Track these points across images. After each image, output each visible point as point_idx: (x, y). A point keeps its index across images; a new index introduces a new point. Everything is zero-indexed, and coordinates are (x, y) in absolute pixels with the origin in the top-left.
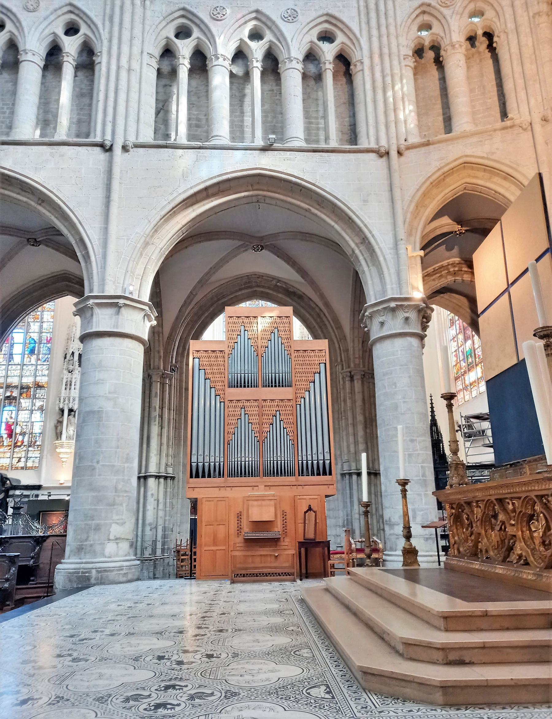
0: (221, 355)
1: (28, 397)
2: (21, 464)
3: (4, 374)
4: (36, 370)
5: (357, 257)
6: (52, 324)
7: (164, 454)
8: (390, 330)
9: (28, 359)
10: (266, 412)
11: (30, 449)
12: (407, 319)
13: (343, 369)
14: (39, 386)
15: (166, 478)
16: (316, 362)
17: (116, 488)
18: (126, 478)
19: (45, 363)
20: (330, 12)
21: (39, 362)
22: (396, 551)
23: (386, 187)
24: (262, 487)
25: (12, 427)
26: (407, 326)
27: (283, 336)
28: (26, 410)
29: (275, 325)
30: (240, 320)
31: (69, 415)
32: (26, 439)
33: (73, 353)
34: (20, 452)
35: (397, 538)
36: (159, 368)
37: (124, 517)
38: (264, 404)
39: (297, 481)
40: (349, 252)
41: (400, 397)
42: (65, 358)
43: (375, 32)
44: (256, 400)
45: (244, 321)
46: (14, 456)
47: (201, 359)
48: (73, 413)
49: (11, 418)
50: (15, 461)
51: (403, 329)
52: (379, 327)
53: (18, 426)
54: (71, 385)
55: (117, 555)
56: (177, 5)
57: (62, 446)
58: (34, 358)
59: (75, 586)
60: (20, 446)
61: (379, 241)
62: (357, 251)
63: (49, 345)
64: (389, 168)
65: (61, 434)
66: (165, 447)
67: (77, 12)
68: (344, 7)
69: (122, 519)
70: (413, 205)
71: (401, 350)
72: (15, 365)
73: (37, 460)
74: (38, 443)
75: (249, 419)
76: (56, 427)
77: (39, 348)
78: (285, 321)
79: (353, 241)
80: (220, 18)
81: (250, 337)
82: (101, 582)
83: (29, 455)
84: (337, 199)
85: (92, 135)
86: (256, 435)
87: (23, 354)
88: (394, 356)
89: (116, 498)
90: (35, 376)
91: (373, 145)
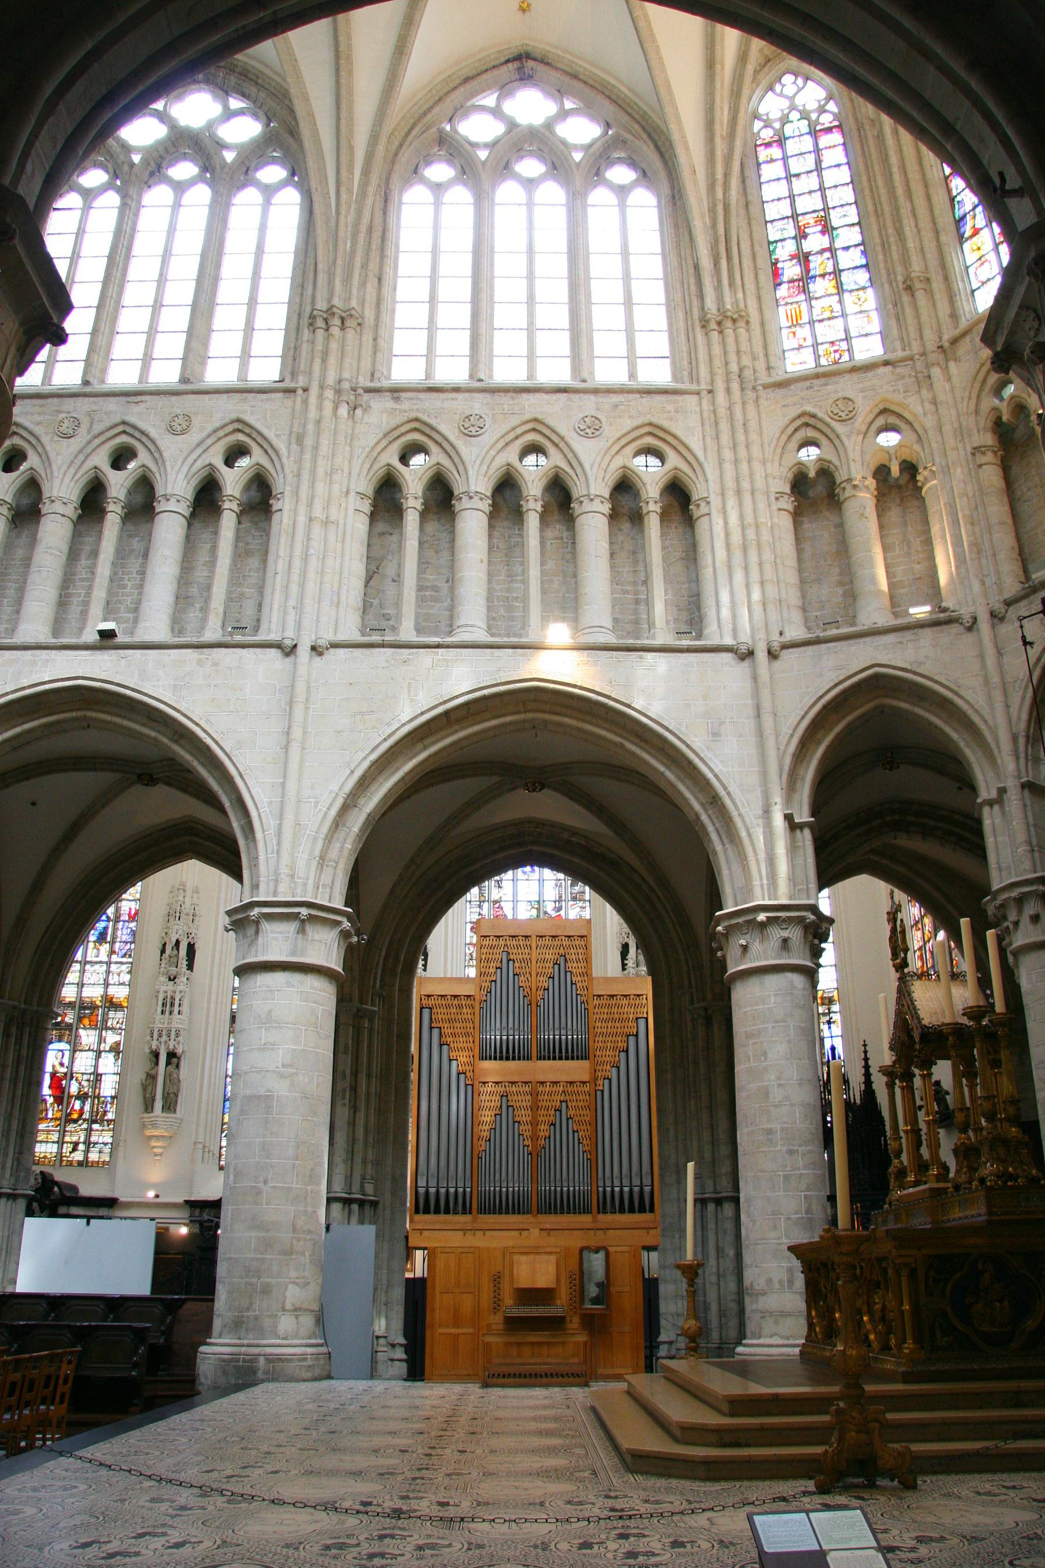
0: (469, 1002)
1: (93, 1026)
2: (78, 1156)
4: (108, 972)
5: (703, 827)
7: (358, 1159)
8: (758, 959)
10: (544, 1103)
11: (95, 1126)
12: (785, 941)
13: (692, 1002)
14: (111, 1004)
15: (362, 1203)
16: (631, 1016)
17: (294, 1226)
18: (310, 1209)
19: (124, 960)
20: (655, 421)
21: (114, 958)
22: (760, 1338)
23: (751, 711)
24: (535, 1232)
25: (64, 1082)
26: (784, 954)
27: (574, 971)
28: (89, 1050)
29: (562, 951)
30: (502, 942)
31: (168, 1063)
32: (87, 1108)
33: (178, 943)
34: (76, 1133)
35: (762, 1318)
36: (351, 1000)
37: (306, 1274)
38: (540, 1089)
39: (595, 1221)
40: (691, 817)
41: (773, 1077)
42: (163, 951)
43: (728, 454)
44: (526, 1083)
45: (508, 943)
46: (67, 1139)
47: (434, 1010)
48: (175, 1060)
50: (67, 1148)
51: (780, 957)
52: (739, 953)
53: (73, 1082)
54: (172, 1005)
55: (296, 1336)
56: (406, 414)
57: (154, 1125)
58: (105, 948)
59: (233, 1382)
60: (75, 1121)
61: (740, 805)
62: (704, 817)
63: (133, 925)
64: (755, 678)
65: (154, 1100)
66: (359, 1146)
67: (247, 430)
68: (677, 411)
69: (304, 1277)
70: (795, 741)
71: (775, 995)
73: (107, 1149)
74: (110, 1116)
75: (514, 1116)
76: (144, 1088)
77: (115, 929)
78: (577, 943)
79: (697, 798)
80: (474, 433)
81: (517, 971)
82: (273, 1377)
83: (93, 1139)
84: (667, 729)
85: (264, 627)
86: (526, 1143)
88: (764, 1004)
89: (295, 1242)
90: (107, 984)
91: (728, 641)
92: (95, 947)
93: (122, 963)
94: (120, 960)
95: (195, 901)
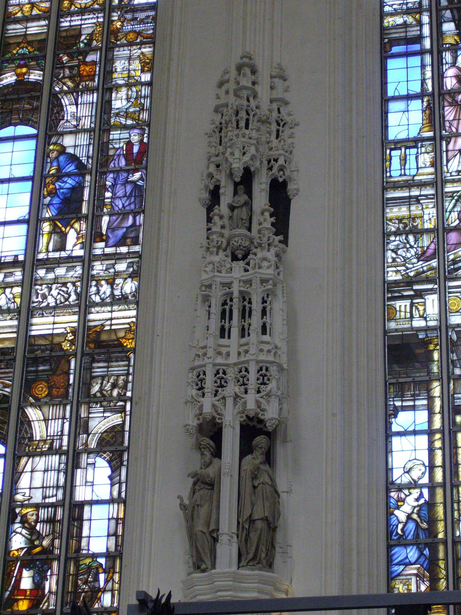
6: (145, 91)
9: (55, 237)
28: (51, 451)
48: (260, 440)
53: (17, 526)
65: (216, 540)
92: (54, 231)
93: (118, 257)
94: (109, 250)
95: (278, 93)
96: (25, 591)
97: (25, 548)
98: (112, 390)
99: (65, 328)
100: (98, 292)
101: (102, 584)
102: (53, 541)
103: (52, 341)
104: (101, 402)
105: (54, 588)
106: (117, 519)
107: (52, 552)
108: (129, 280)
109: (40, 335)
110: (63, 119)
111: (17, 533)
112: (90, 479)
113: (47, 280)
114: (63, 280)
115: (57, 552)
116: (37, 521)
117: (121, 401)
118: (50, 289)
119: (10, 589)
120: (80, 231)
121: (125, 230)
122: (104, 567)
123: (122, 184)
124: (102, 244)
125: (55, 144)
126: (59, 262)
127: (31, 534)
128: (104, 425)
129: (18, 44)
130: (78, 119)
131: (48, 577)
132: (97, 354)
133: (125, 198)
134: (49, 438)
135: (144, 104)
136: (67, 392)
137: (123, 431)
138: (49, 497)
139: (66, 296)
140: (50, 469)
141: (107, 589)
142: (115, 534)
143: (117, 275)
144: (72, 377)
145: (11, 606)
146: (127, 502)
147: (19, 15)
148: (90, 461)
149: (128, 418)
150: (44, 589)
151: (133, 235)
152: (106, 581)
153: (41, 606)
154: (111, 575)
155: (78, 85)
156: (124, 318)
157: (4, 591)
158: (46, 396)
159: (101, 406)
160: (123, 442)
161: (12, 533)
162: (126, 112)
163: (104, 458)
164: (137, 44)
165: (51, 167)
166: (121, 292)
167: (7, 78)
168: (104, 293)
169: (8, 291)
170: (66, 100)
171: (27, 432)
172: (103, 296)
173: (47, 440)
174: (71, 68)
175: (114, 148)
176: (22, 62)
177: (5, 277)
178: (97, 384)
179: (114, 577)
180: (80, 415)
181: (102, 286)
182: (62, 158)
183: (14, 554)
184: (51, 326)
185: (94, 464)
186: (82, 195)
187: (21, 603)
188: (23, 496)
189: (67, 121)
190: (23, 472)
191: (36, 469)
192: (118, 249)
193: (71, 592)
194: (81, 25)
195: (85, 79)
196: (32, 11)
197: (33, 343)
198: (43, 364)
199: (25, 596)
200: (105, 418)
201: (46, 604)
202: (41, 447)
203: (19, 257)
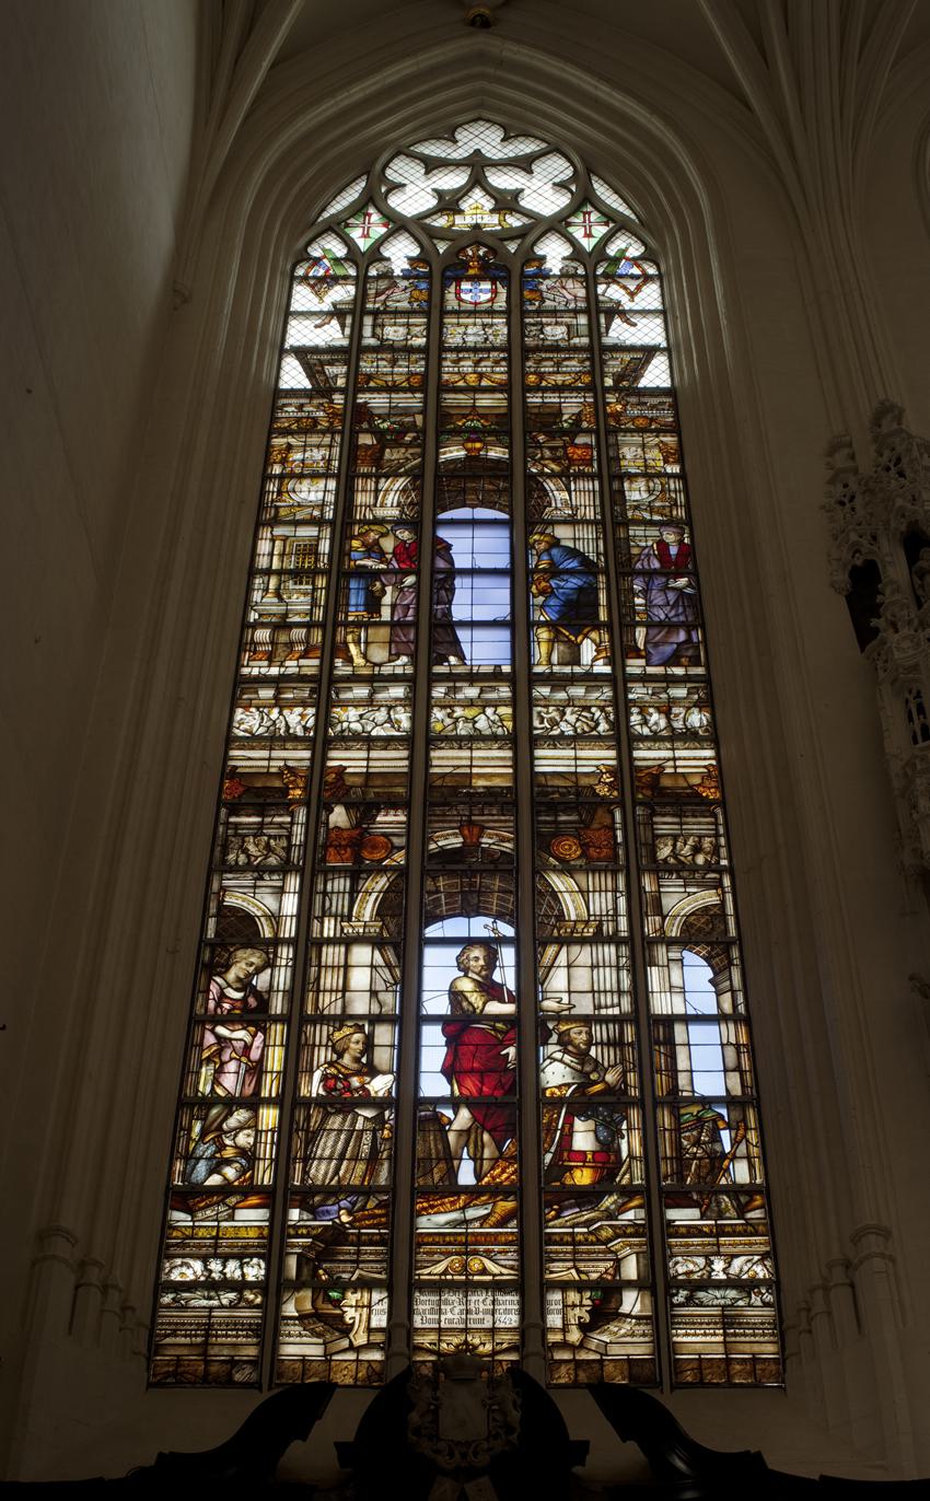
3: (406, 725)
4: (621, 705)
21: (635, 666)
28: (599, 939)
46: (561, 1271)
49: (491, 990)
50: (562, 1314)
60: (587, 1197)
72: (472, 678)
87: (518, 626)
96: (584, 1153)
97: (573, 1084)
98: (694, 855)
99: (597, 767)
100: (645, 722)
101: (728, 1149)
102: (624, 1074)
103: (577, 783)
104: (678, 872)
105: (638, 1150)
106: (737, 1046)
107: (625, 1092)
108: (696, 710)
109: (554, 772)
110: (550, 506)
111: (555, 1060)
112: (676, 980)
113: (555, 700)
114: (583, 703)
115: (633, 1092)
116: (589, 1043)
117: (713, 871)
118: (563, 714)
119: (553, 1150)
120: (601, 642)
121: (675, 646)
122: (726, 1119)
123: (660, 590)
124: (642, 662)
125: (542, 533)
126: (573, 679)
127: (582, 1064)
128: (689, 905)
129: (464, 416)
130: (575, 508)
131: (625, 1132)
132: (657, 804)
133: (668, 608)
134: (592, 918)
135: (676, 499)
136: (616, 856)
137: (724, 915)
138: (606, 1007)
139: (592, 724)
140: (601, 964)
141: (738, 1155)
142: (738, 1069)
143: (674, 703)
144: (619, 833)
145: (560, 1178)
146: (754, 1020)
147: (461, 384)
148: (672, 955)
149: (729, 897)
150: (619, 1151)
151: (690, 653)
152: (735, 1143)
153: (618, 1179)
154: (741, 1132)
155: (568, 468)
156: (695, 759)
157: (543, 1152)
158: (579, 858)
159: (679, 877)
160: (726, 930)
161: (544, 1060)
162: (649, 506)
163: (697, 953)
164: (652, 431)
165: (538, 561)
166: (685, 724)
167: (451, 452)
168: (656, 723)
169: (489, 711)
170: (552, 485)
171: (552, 908)
172: (654, 728)
173: (589, 921)
174: (551, 449)
175: (638, 546)
176: (473, 436)
177: (482, 692)
178: (666, 845)
179: (749, 1136)
180: (644, 888)
181: (651, 715)
182: (555, 552)
183: (553, 1093)
184: (573, 762)
185: (681, 960)
186: (597, 598)
187: (577, 1173)
188: (558, 1002)
189: (556, 508)
190: (552, 966)
191: (575, 963)
192: (668, 669)
193: (671, 1158)
194: (560, 403)
195: (577, 462)
196: (480, 381)
197: (544, 782)
198: (565, 812)
199: (585, 1161)
200: (689, 894)
201: (627, 1176)
202: (580, 930)
203: (503, 667)
